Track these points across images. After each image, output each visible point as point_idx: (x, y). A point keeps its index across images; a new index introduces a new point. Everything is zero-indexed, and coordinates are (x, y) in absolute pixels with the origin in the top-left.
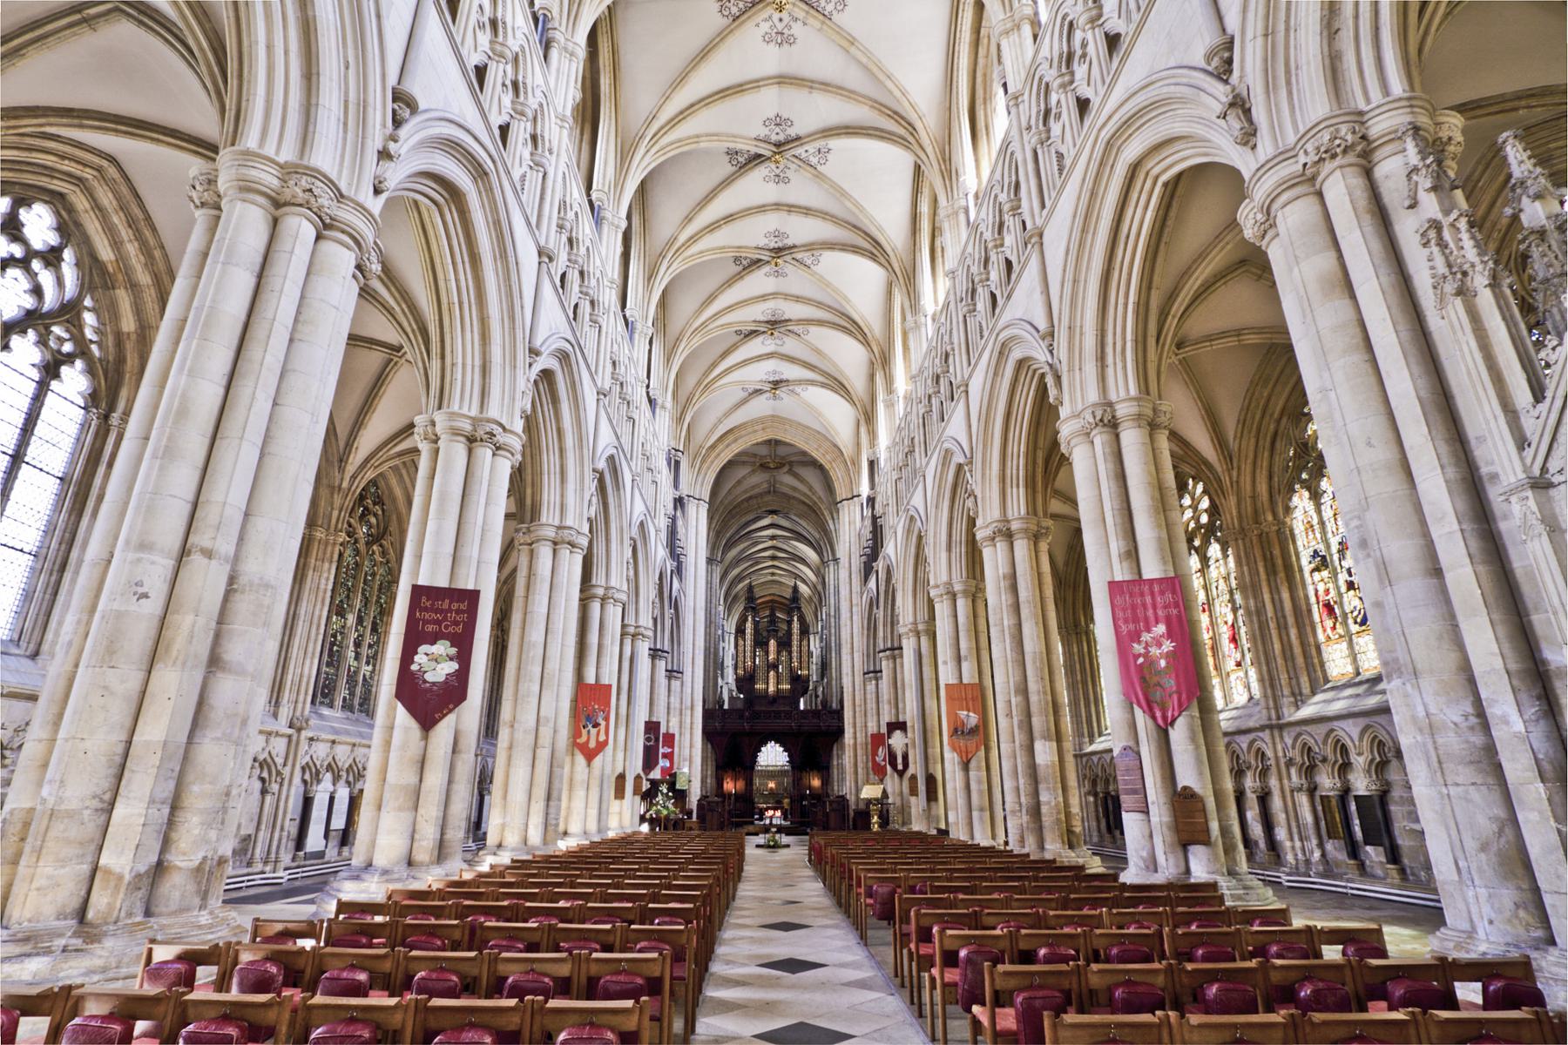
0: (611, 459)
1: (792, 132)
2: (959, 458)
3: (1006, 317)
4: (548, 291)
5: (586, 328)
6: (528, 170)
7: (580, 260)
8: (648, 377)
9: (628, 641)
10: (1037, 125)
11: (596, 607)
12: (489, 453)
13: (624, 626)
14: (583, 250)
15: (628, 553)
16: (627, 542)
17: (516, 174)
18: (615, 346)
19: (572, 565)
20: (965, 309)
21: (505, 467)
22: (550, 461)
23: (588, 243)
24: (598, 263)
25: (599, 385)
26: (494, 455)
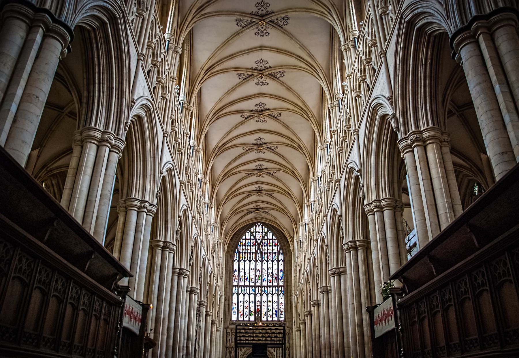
0: (169, 171)
1: (270, 9)
2: (355, 173)
3: (374, 95)
4: (141, 76)
5: (159, 100)
6: (135, 17)
7: (158, 64)
8: (190, 131)
9: (176, 278)
10: (381, 5)
11: (159, 252)
12: (108, 149)
13: (174, 268)
14: (160, 59)
15: (177, 227)
16: (176, 220)
17: (131, 19)
18: (174, 112)
19: (146, 220)
20: (355, 94)
21: (116, 157)
22: (138, 167)
23: (162, 56)
24: (167, 68)
25: (165, 129)
26: (110, 151)
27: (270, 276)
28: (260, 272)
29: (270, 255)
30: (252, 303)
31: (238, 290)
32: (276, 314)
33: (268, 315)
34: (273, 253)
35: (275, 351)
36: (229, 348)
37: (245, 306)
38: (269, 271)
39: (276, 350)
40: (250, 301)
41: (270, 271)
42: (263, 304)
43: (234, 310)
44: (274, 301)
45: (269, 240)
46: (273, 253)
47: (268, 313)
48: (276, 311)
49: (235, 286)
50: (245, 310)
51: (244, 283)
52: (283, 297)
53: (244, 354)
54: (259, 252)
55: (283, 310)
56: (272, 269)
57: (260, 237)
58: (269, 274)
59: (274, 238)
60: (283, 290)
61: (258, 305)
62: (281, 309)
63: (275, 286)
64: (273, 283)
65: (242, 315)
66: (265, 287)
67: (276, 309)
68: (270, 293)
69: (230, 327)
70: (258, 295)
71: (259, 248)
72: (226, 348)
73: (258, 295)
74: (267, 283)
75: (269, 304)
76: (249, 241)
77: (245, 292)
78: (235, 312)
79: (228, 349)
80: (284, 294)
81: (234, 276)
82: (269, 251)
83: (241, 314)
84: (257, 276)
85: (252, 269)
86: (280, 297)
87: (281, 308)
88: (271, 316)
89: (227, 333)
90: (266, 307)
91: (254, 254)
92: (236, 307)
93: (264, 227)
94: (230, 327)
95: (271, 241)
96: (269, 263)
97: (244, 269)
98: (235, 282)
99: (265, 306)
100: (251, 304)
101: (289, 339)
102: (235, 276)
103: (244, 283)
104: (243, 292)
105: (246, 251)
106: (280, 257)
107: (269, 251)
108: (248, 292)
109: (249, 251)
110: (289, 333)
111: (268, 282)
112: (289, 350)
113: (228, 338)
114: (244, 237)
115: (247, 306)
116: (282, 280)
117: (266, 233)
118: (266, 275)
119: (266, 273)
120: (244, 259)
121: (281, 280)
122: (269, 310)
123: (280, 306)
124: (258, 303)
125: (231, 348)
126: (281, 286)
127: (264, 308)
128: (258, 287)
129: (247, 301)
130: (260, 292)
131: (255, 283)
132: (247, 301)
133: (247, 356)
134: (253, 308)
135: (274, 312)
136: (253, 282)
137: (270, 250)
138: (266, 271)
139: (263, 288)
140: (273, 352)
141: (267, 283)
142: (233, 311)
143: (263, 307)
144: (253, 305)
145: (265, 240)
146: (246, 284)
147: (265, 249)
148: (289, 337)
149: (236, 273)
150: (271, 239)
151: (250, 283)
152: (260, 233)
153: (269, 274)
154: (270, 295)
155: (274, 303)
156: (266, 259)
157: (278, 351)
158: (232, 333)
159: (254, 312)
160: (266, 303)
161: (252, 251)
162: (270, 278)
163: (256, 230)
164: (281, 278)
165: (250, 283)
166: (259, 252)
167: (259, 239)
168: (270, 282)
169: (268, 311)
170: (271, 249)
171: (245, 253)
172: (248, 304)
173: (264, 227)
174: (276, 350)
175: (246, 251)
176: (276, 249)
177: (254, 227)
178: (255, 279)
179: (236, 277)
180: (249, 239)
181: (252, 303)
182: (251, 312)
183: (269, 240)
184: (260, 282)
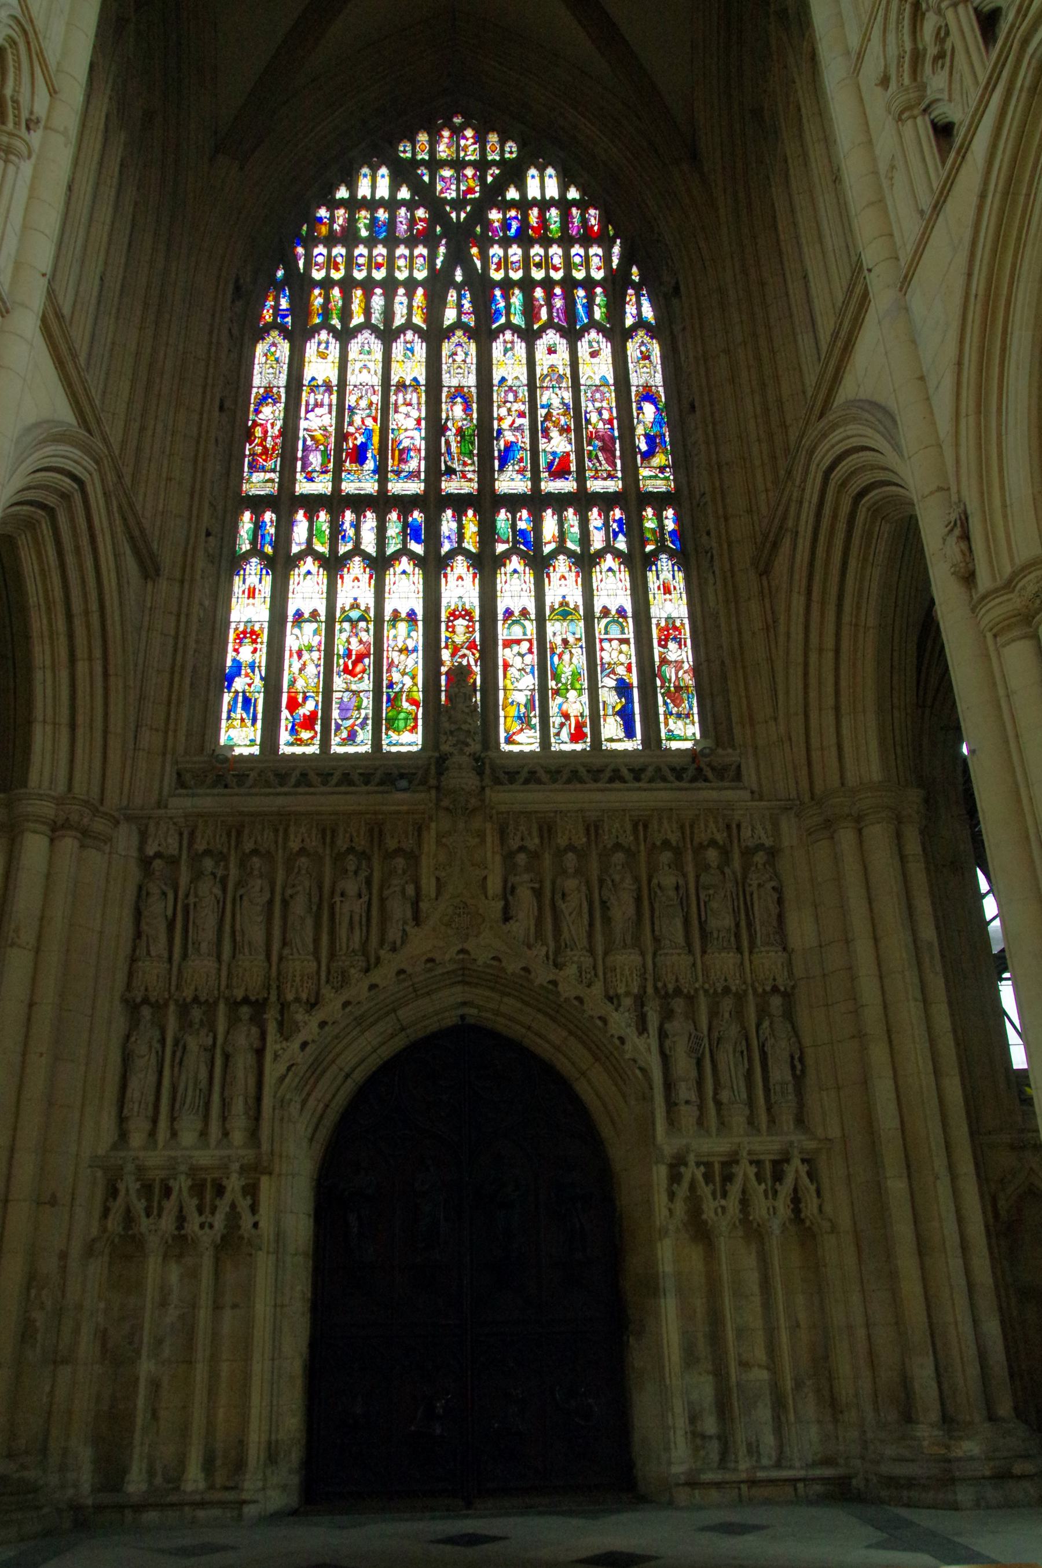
27: (554, 433)
28: (467, 408)
29: (550, 296)
30: (402, 627)
31: (285, 527)
32: (625, 715)
33: (556, 720)
34: (569, 284)
35: (642, 1028)
36: (159, 1008)
37: (340, 648)
38: (545, 397)
39: (653, 1020)
40: (388, 614)
41: (554, 398)
42: (503, 633)
43: (239, 684)
44: (606, 612)
45: (534, 213)
46: (569, 284)
47: (554, 705)
48: (623, 688)
49: (258, 505)
50: (338, 683)
51: (337, 481)
52: (680, 576)
53: (316, 1069)
54: (459, 276)
55: (689, 680)
56: (567, 383)
57: (470, 190)
58: (548, 416)
59: (573, 194)
60: (670, 525)
61: (459, 639)
62: (670, 672)
63: (606, 502)
64: (581, 479)
65: (308, 722)
66: (514, 502)
67: (621, 670)
68: (561, 549)
69: (181, 804)
70: (460, 565)
71: (458, 257)
72: (132, 1007)
73: (460, 565)
74: (536, 479)
75: (555, 630)
76: (382, 215)
77: (343, 549)
78: (247, 702)
79: (146, 1012)
80: (682, 559)
81: (249, 436)
82: (538, 275)
83: (302, 711)
84: (451, 434)
85: (402, 386)
86: (651, 576)
87: (664, 661)
88: (579, 726)
89: (145, 863)
90: (531, 659)
91: (420, 291)
92: (261, 658)
93: (493, 138)
94: (181, 804)
95: (554, 214)
96: (541, 345)
97: (335, 382)
98: (258, 477)
99: (525, 646)
100: (398, 635)
101: (780, 901)
102: (258, 432)
103: (337, 481)
104: (321, 548)
105: (359, 275)
106: (630, 310)
107: (538, 275)
108: (369, 544)
109: (379, 275)
110: (773, 853)
111: (544, 475)
112: (789, 1014)
113: (157, 909)
114: (343, 193)
115: (355, 646)
116: (659, 460)
117: (514, 173)
118: (525, 422)
119: (524, 408)
120: (335, 322)
121: (648, 455)
122: (556, 677)
123: (657, 650)
124: (461, 624)
125: (184, 1009)
126: (659, 501)
127: (518, 662)
128: (460, 503)
129: (355, 614)
130: (471, 544)
131: (435, 472)
132: (355, 614)
133: (350, 1086)
134: (415, 662)
135: (609, 697)
136: (413, 475)
137: (546, 263)
138: (523, 393)
139: (503, 517)
140: (631, 1034)
141: (536, 479)
142: (227, 698)
143: (504, 654)
144: (417, 638)
145: (505, 206)
146: (349, 487)
147: (504, 263)
148: (778, 890)
149: (271, 415)
150: (553, 203)
151: (383, 481)
152: (469, 172)
153: (548, 416)
154: (562, 564)
155: (600, 627)
156: (517, 320)
157: (675, 1026)
158: (196, 859)
159: (419, 696)
160: (531, 628)
161: (401, 275)
162: (559, 444)
163: (433, 152)
164: (650, 439)
165: (383, 481)
166: (459, 276)
167: (458, 204)
168: (560, 471)
169: (552, 684)
170: (557, 261)
171: (347, 285)
172: (368, 637)
173: (493, 138)
174: (653, 1020)
175: (359, 275)
176: (595, 262)
177: (423, 138)
178: (433, 455)
179: (269, 442)
180: (382, 203)
181: (402, 627)
182: (393, 701)
183: (534, 213)
184: (471, 470)
